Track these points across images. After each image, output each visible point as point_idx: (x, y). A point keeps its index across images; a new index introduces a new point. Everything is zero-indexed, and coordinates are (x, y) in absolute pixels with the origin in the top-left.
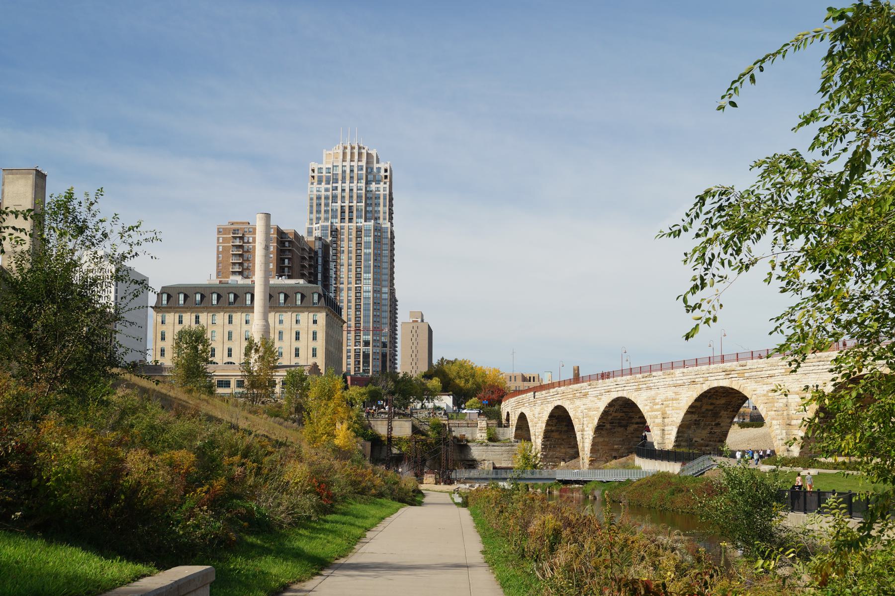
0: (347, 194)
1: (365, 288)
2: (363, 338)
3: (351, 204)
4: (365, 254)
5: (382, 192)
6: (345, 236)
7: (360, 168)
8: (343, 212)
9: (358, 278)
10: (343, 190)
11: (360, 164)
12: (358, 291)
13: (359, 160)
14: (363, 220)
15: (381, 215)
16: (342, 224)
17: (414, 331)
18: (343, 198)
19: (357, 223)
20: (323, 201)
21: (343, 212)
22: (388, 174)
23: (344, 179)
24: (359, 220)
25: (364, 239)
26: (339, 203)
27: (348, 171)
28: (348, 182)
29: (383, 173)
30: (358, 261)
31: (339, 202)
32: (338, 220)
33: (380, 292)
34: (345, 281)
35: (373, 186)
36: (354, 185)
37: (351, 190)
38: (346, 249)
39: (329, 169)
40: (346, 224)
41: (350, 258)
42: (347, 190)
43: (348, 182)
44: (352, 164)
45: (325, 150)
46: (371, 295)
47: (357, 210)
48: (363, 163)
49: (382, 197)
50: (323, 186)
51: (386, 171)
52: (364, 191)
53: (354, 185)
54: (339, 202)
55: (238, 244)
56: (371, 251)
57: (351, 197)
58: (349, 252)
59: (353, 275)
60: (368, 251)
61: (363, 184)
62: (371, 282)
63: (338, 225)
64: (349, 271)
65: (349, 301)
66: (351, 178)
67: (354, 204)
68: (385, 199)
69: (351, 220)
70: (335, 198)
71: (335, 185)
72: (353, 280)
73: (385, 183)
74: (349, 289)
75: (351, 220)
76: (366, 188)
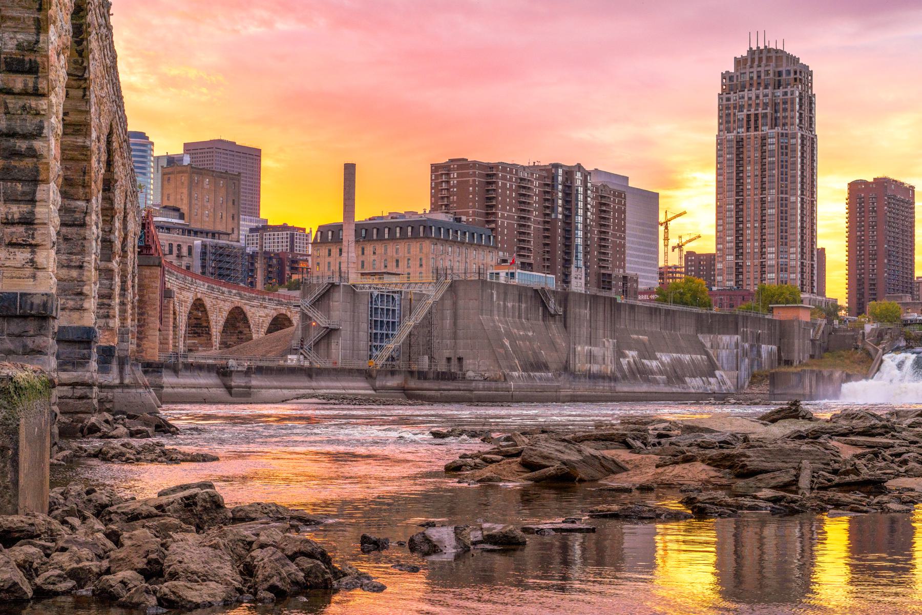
4: (770, 163)
10: (750, 99)
16: (748, 134)
18: (750, 105)
19: (762, 131)
21: (748, 121)
27: (755, 78)
49: (789, 102)
54: (745, 111)
66: (759, 84)
67: (760, 111)
69: (756, 129)
75: (756, 129)
76: (773, 93)
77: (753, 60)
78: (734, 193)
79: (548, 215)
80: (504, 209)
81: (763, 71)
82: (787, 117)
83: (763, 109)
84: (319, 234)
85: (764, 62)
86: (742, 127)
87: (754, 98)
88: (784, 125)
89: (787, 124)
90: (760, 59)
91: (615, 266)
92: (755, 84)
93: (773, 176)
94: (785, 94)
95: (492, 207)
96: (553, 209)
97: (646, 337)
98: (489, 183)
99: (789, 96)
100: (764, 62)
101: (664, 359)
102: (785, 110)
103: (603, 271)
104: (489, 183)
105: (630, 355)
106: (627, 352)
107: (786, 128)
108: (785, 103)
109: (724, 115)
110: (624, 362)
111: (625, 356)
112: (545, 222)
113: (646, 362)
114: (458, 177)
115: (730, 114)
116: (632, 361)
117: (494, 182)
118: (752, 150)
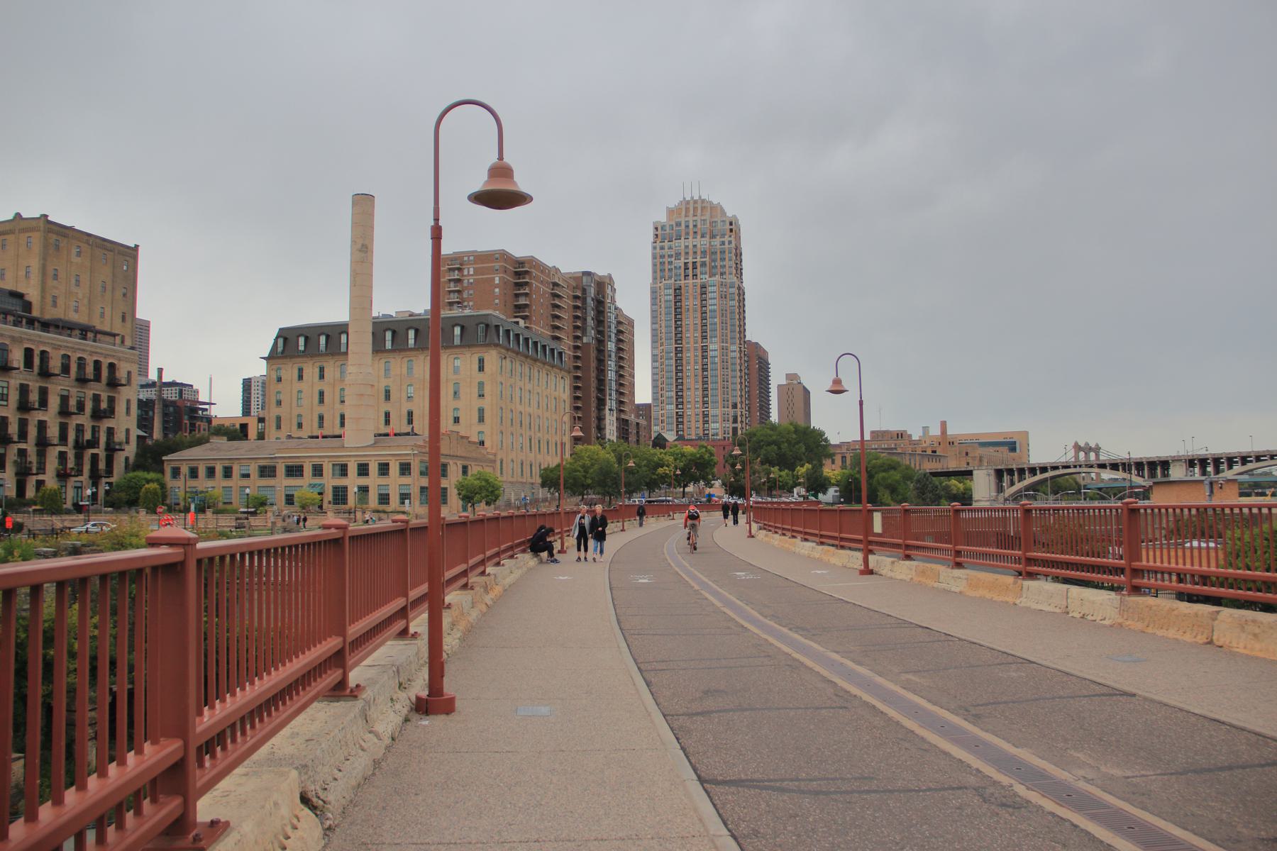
1: (711, 347)
14: (707, 276)
17: (789, 393)
19: (701, 279)
21: (686, 268)
26: (683, 260)
27: (691, 226)
31: (682, 259)
39: (672, 225)
40: (690, 281)
48: (707, 217)
54: (682, 259)
55: (456, 277)
57: (695, 253)
69: (695, 276)
73: (730, 236)
74: (696, 349)
76: (710, 243)
77: (687, 210)
79: (577, 338)
81: (699, 221)
82: (725, 266)
83: (701, 258)
84: (281, 341)
85: (699, 211)
87: (691, 246)
88: (722, 274)
89: (725, 273)
90: (695, 209)
92: (691, 233)
93: (715, 324)
94: (723, 243)
96: (584, 330)
98: (518, 285)
99: (727, 245)
100: (699, 211)
102: (723, 259)
104: (518, 285)
107: (724, 277)
108: (723, 252)
109: (658, 264)
115: (664, 263)
117: (526, 284)
118: (691, 298)
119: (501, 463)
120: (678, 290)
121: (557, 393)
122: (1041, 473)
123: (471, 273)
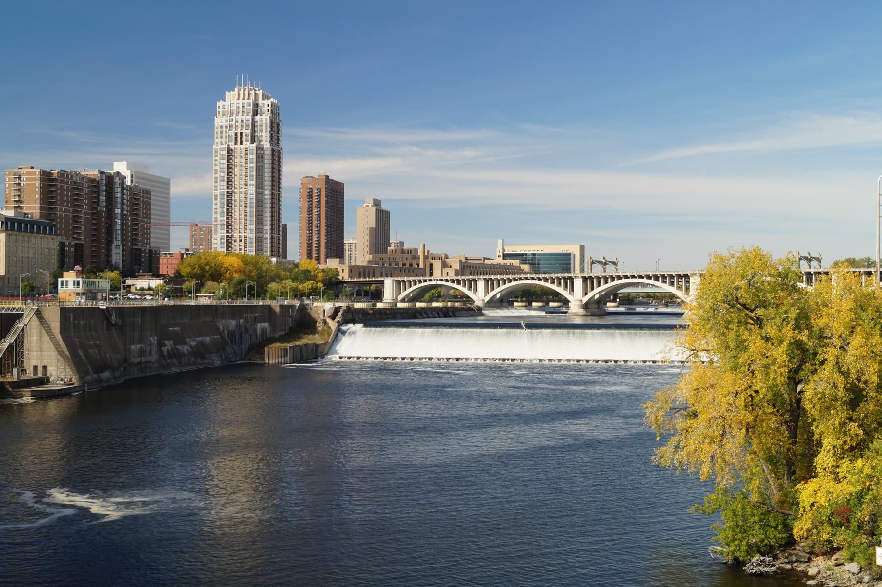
0: (239, 124)
2: (249, 227)
3: (241, 131)
4: (251, 167)
5: (264, 122)
6: (237, 155)
7: (249, 105)
8: (236, 138)
9: (246, 185)
10: (237, 121)
11: (249, 101)
12: (246, 193)
13: (249, 99)
15: (263, 138)
16: (236, 146)
18: (236, 126)
20: (224, 130)
21: (236, 138)
22: (270, 108)
23: (238, 113)
24: (247, 143)
25: (249, 156)
26: (232, 133)
27: (241, 107)
28: (240, 115)
29: (266, 108)
30: (246, 172)
31: (234, 130)
32: (233, 143)
33: (262, 193)
34: (238, 187)
35: (258, 118)
36: (244, 118)
37: (242, 121)
38: (238, 164)
40: (238, 146)
41: (240, 170)
42: (239, 121)
43: (240, 115)
44: (244, 101)
45: (227, 92)
46: (254, 196)
47: (245, 135)
50: (225, 118)
51: (268, 106)
52: (250, 122)
53: (244, 118)
54: (234, 130)
56: (254, 165)
57: (242, 126)
58: (240, 166)
59: (243, 182)
60: (252, 165)
61: (250, 117)
62: (254, 187)
63: (232, 146)
64: (240, 179)
65: (240, 201)
66: (243, 112)
68: (266, 127)
69: (241, 143)
70: (231, 127)
71: (231, 117)
72: (243, 186)
74: (240, 192)
78: (226, 187)
80: (62, 204)
86: (232, 141)
91: (143, 243)
93: (253, 176)
95: (51, 203)
96: (98, 203)
97: (179, 328)
101: (192, 343)
103: (135, 247)
105: (168, 344)
106: (166, 342)
110: (164, 349)
111: (165, 345)
112: (93, 214)
113: (179, 347)
114: (27, 181)
116: (170, 348)
119: (9, 279)
120: (230, 152)
121: (48, 246)
122: (509, 282)
123: (25, 180)
